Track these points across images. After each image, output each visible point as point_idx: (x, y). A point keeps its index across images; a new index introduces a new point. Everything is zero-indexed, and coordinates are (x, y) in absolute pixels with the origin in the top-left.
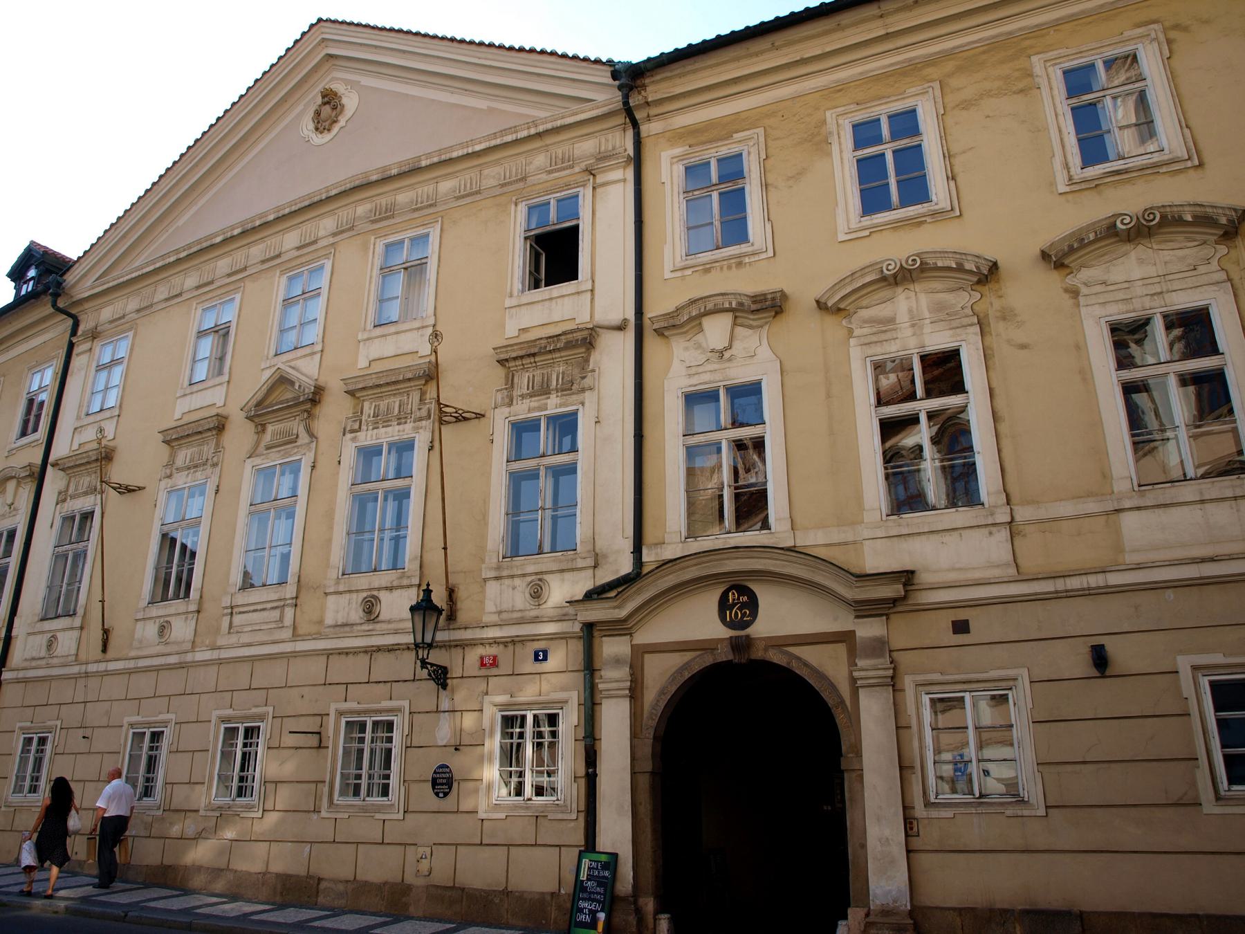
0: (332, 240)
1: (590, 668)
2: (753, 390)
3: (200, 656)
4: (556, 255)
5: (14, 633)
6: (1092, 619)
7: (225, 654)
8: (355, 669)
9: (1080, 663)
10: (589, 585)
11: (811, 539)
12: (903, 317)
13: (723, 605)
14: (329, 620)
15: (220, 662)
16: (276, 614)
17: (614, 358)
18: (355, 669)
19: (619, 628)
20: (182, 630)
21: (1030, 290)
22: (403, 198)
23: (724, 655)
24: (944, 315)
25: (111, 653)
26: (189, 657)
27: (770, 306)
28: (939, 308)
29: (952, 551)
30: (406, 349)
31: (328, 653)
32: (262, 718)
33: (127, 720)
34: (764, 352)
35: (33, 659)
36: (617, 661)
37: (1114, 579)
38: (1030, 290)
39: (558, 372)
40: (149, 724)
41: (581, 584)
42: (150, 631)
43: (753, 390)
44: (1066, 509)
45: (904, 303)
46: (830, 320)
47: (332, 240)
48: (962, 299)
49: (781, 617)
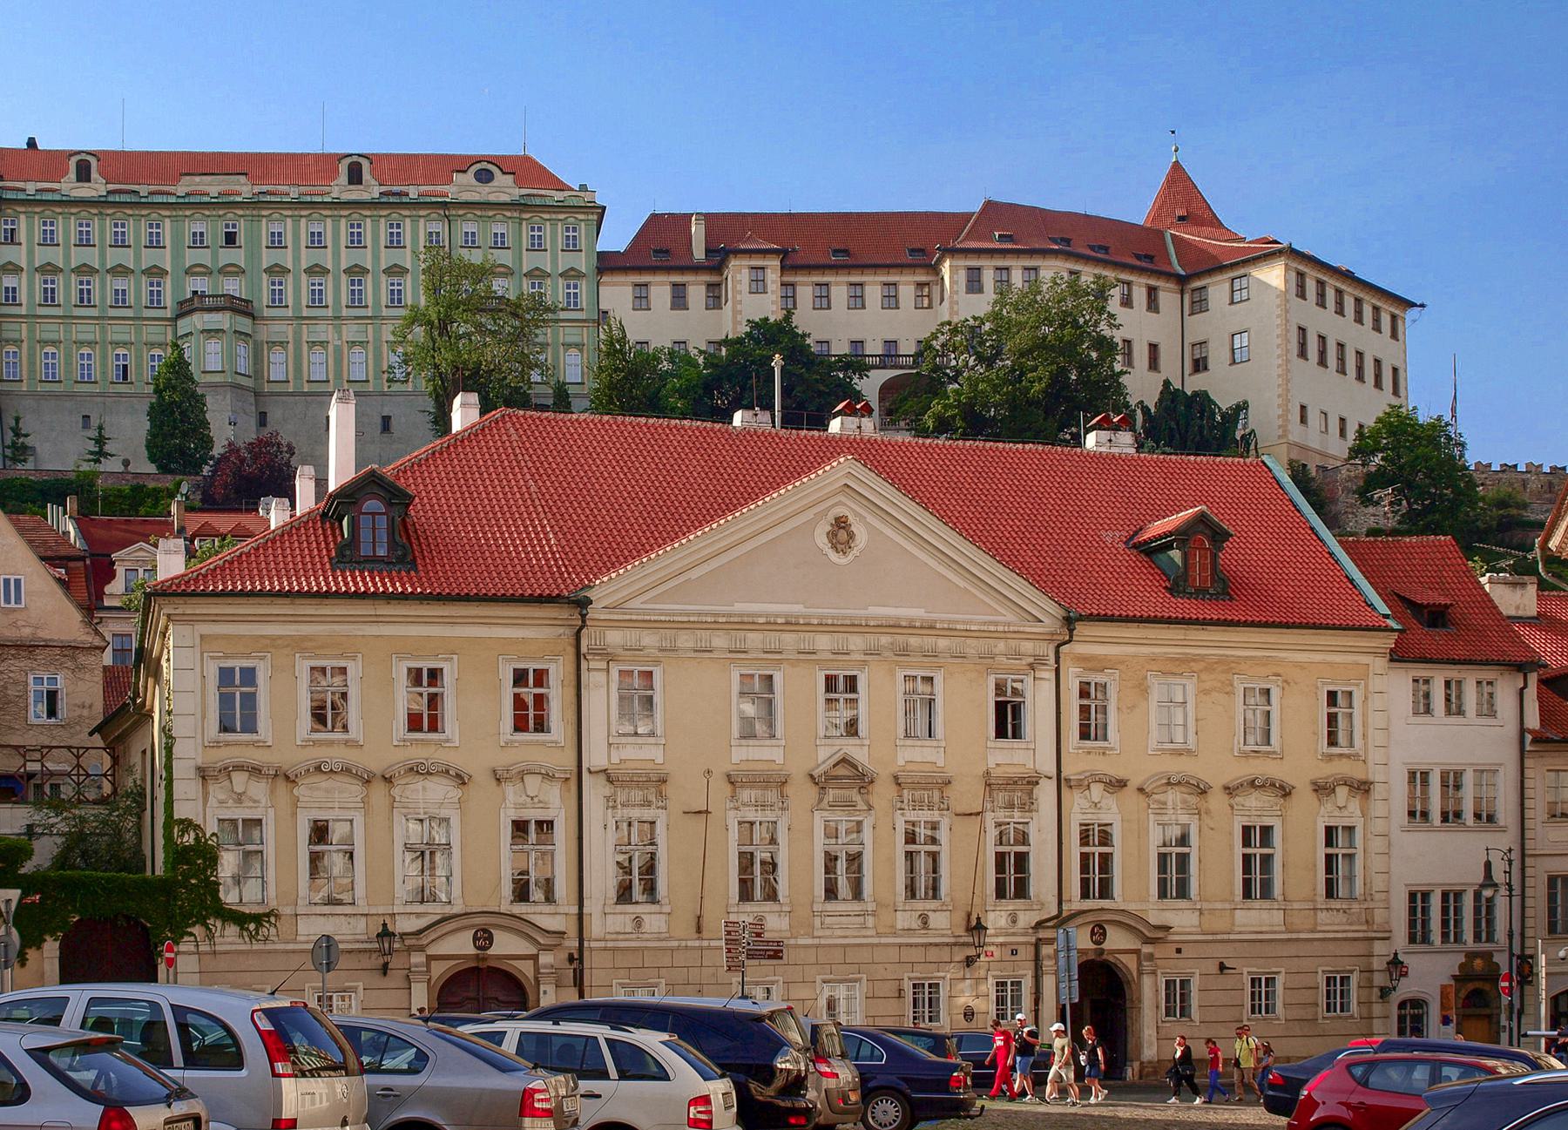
0: (863, 657)
1: (1037, 959)
3: (801, 941)
4: (1008, 719)
6: (1221, 952)
7: (823, 941)
8: (916, 955)
9: (1215, 970)
10: (1038, 919)
11: (1131, 907)
12: (1170, 804)
13: (1093, 933)
14: (899, 926)
15: (817, 946)
17: (1046, 793)
18: (916, 955)
21: (1217, 801)
22: (914, 641)
23: (1091, 956)
24: (1187, 807)
25: (705, 934)
28: (1184, 802)
29: (1180, 918)
31: (900, 945)
34: (1115, 808)
36: (1049, 957)
37: (1232, 937)
38: (1217, 801)
39: (1018, 796)
41: (1035, 917)
44: (1219, 906)
45: (1173, 797)
46: (1142, 797)
47: (863, 657)
48: (1193, 800)
49: (1117, 940)
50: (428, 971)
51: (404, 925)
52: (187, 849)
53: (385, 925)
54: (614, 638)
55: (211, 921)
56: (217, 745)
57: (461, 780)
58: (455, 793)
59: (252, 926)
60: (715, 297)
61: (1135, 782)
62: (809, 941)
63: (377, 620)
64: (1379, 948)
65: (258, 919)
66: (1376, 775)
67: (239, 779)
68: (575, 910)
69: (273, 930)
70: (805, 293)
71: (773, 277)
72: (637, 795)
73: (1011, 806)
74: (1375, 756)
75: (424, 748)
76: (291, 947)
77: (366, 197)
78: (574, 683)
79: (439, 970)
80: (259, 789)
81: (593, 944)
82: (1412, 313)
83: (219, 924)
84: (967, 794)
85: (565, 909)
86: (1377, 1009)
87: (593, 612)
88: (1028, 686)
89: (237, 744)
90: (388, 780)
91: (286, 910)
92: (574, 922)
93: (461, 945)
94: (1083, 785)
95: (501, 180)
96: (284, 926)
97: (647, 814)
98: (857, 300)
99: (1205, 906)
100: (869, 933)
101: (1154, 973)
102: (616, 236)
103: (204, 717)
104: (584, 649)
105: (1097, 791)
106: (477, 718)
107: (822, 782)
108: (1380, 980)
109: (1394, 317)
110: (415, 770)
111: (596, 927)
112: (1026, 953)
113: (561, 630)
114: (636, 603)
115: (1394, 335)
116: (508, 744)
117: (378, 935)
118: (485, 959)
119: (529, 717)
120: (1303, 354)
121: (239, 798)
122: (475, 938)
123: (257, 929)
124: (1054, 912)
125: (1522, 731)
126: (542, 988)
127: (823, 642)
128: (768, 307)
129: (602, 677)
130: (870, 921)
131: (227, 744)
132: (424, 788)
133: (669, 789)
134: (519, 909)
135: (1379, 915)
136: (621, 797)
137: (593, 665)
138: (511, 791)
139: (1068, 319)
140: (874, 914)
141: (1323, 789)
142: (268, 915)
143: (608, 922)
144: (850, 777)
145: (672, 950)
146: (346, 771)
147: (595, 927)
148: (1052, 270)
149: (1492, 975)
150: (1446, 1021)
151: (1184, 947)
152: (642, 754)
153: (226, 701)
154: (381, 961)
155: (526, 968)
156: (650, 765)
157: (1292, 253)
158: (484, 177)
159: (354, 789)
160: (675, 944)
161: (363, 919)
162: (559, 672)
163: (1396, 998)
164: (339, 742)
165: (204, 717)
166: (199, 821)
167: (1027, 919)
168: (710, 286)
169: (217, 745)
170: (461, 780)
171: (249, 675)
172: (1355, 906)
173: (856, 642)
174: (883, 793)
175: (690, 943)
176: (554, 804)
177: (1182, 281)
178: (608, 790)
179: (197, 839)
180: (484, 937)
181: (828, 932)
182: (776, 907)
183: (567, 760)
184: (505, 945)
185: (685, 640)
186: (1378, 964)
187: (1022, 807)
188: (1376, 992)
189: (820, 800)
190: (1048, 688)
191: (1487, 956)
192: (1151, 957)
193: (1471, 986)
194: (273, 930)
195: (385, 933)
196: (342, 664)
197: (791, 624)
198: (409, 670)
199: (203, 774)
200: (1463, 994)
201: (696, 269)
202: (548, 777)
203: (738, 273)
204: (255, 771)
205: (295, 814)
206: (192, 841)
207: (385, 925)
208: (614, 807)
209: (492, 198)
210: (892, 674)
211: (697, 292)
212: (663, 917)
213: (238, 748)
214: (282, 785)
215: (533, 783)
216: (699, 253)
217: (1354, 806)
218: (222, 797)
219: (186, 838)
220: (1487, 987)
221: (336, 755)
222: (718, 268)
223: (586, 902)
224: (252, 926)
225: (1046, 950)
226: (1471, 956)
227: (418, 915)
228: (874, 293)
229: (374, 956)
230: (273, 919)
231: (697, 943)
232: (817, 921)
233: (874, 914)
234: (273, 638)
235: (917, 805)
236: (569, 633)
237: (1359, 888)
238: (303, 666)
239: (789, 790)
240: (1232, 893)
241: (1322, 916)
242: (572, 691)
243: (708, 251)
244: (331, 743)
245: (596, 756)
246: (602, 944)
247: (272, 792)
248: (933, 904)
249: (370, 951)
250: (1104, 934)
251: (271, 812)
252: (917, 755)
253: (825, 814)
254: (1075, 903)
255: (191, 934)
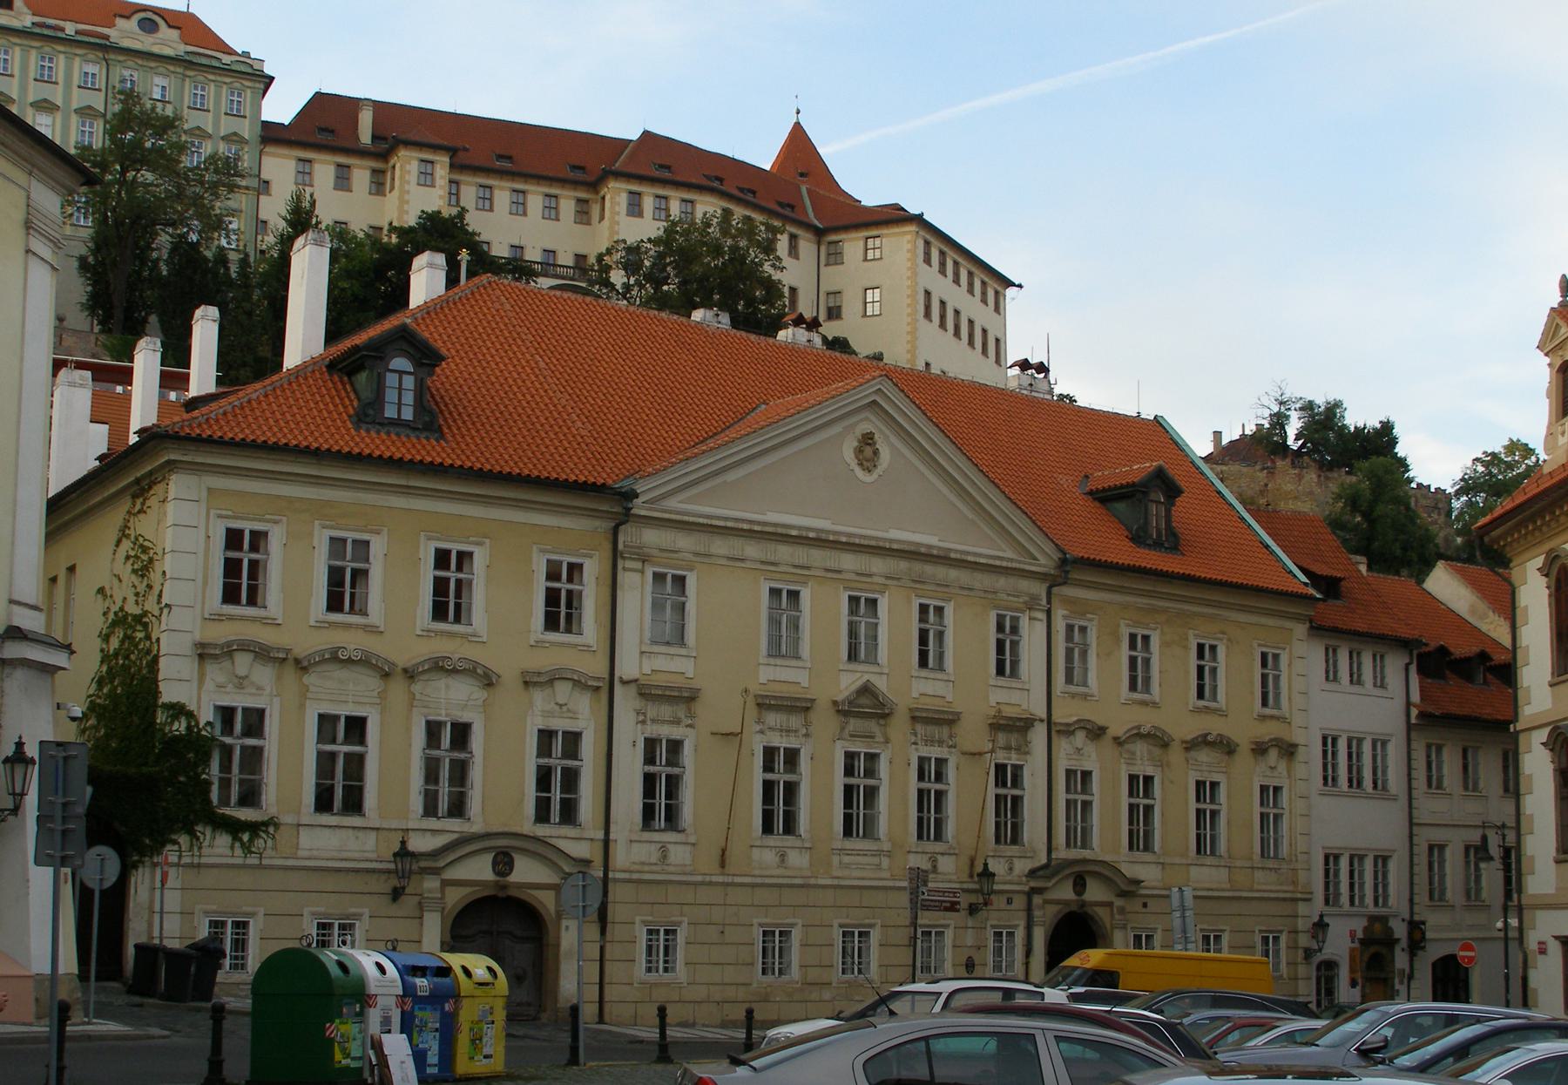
1: (1029, 909)
2: (1086, 775)
3: (821, 882)
5: (612, 836)
11: (1107, 858)
16: (876, 860)
17: (1038, 736)
19: (1039, 891)
20: (798, 860)
26: (812, 881)
27: (1096, 733)
29: (1146, 871)
30: (940, 693)
32: (871, 926)
33: (755, 921)
34: (1094, 755)
35: (643, 863)
40: (777, 925)
42: (769, 857)
43: (1086, 775)
44: (1177, 860)
45: (1140, 748)
48: (1157, 751)
49: (1095, 892)
50: (442, 898)
51: (418, 844)
52: (177, 739)
53: (403, 843)
54: (652, 538)
55: (199, 828)
56: (218, 618)
57: (488, 680)
58: (480, 694)
59: (246, 837)
60: (379, 185)
61: (1112, 732)
62: (829, 882)
63: (406, 491)
64: (1302, 908)
65: (255, 828)
66: (1298, 737)
67: (243, 662)
68: (600, 835)
69: (270, 842)
70: (469, 195)
71: (442, 172)
72: (666, 711)
73: (1008, 748)
74: (1298, 719)
75: (447, 642)
76: (290, 863)
77: (16, 24)
78: (609, 581)
79: (455, 897)
80: (263, 675)
81: (619, 875)
82: (1011, 292)
83: (208, 832)
84: (972, 734)
85: (590, 834)
86: (1302, 970)
87: (639, 508)
88: (1024, 623)
89: (242, 618)
90: (410, 674)
91: (287, 819)
92: (599, 847)
93: (480, 870)
94: (1068, 731)
95: (165, 32)
96: (283, 835)
97: (675, 732)
98: (520, 208)
99: (1168, 860)
100: (886, 875)
101: (1124, 927)
102: (281, 107)
103: (205, 583)
104: (621, 546)
105: (1080, 737)
106: (504, 608)
107: (845, 710)
108: (1304, 940)
109: (997, 293)
110: (440, 667)
111: (621, 857)
112: (1019, 902)
113: (597, 523)
114: (673, 503)
115: (997, 309)
116: (539, 644)
117: (395, 855)
118: (504, 887)
119: (560, 611)
120: (928, 315)
121: (241, 682)
122: (495, 863)
123: (251, 840)
124: (1044, 861)
125: (1408, 704)
126: (564, 923)
127: (848, 561)
128: (434, 200)
129: (636, 577)
130: (885, 862)
131: (231, 618)
132: (447, 687)
133: (698, 707)
134: (542, 831)
135: (1302, 875)
136: (652, 710)
137: (629, 564)
138: (539, 697)
139: (738, 257)
140: (889, 854)
141: (1260, 750)
142: (266, 824)
143: (634, 850)
144: (867, 706)
145: (696, 884)
146: (364, 661)
147: (620, 857)
148: (707, 207)
149: (1391, 942)
150: (1353, 984)
151: (1150, 902)
152: (672, 666)
153: (232, 568)
154: (394, 882)
155: (546, 901)
156: (678, 681)
157: (919, 220)
158: (149, 26)
159: (368, 683)
160: (699, 878)
161: (373, 834)
162: (593, 569)
163: (1319, 958)
164: (357, 626)
165: (205, 583)
166: (192, 707)
167: (1022, 866)
168: (375, 172)
169: (218, 618)
170: (488, 680)
171: (258, 538)
172: (1284, 866)
173: (878, 565)
174: (899, 727)
175: (714, 879)
176: (584, 716)
177: (819, 233)
178: (638, 703)
179: (189, 728)
180: (504, 862)
181: (846, 873)
182: (798, 843)
183: (599, 667)
184: (526, 872)
185: (720, 546)
186: (1302, 924)
187: (1018, 749)
188: (1301, 953)
189: (843, 729)
190: (1041, 628)
191: (1383, 920)
192: (1122, 911)
193: (1373, 949)
194: (270, 842)
195: (403, 853)
196: (365, 537)
197: (821, 541)
198: (437, 550)
199: (204, 653)
200: (1366, 958)
201: (362, 153)
202: (579, 684)
203: (407, 164)
204: (262, 653)
205: (302, 706)
206: (183, 729)
207: (403, 843)
208: (643, 722)
209: (156, 50)
210: (909, 602)
211: (361, 175)
212: (688, 848)
213: (241, 624)
214: (290, 672)
215: (563, 690)
216: (365, 137)
217: (1282, 766)
218: (221, 679)
219: (175, 726)
220: (1384, 951)
221: (352, 642)
222: (384, 156)
223: (613, 828)
224: (246, 837)
225: (1037, 900)
226: (1373, 919)
227: (434, 832)
228: (535, 202)
229: (384, 877)
230: (271, 829)
231: (720, 879)
232: (836, 859)
233: (889, 854)
234: (290, 500)
235: (930, 741)
236: (605, 525)
237: (1285, 850)
238: (321, 539)
239: (813, 715)
240: (1187, 848)
241: (1259, 875)
242: (607, 591)
243: (374, 137)
244: (349, 626)
245: (628, 666)
246: (626, 876)
247: (279, 678)
248: (939, 847)
249: (389, 871)
250: (1084, 885)
251: (276, 701)
252: (926, 689)
253: (846, 744)
254: (1062, 853)
255: (175, 842)
